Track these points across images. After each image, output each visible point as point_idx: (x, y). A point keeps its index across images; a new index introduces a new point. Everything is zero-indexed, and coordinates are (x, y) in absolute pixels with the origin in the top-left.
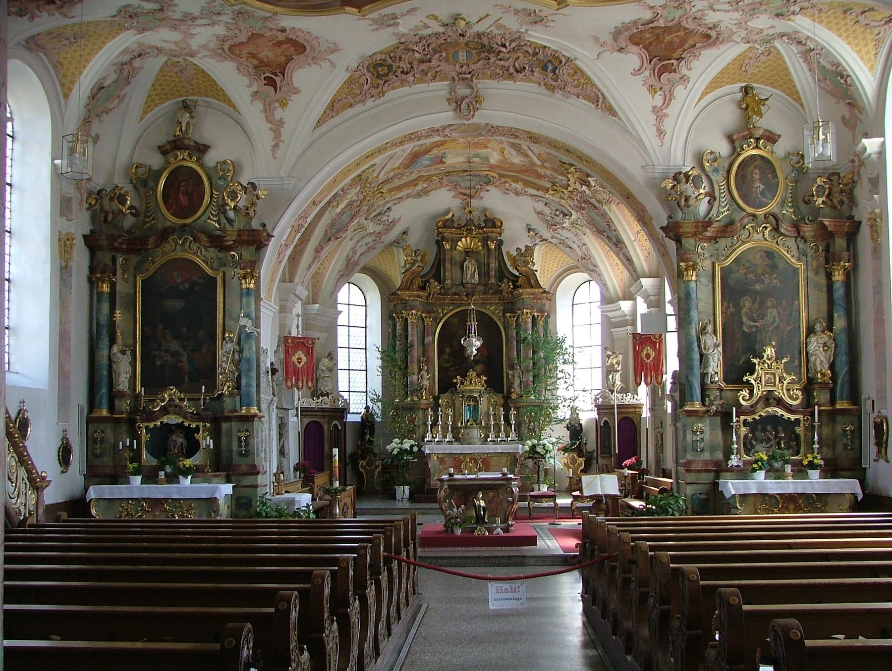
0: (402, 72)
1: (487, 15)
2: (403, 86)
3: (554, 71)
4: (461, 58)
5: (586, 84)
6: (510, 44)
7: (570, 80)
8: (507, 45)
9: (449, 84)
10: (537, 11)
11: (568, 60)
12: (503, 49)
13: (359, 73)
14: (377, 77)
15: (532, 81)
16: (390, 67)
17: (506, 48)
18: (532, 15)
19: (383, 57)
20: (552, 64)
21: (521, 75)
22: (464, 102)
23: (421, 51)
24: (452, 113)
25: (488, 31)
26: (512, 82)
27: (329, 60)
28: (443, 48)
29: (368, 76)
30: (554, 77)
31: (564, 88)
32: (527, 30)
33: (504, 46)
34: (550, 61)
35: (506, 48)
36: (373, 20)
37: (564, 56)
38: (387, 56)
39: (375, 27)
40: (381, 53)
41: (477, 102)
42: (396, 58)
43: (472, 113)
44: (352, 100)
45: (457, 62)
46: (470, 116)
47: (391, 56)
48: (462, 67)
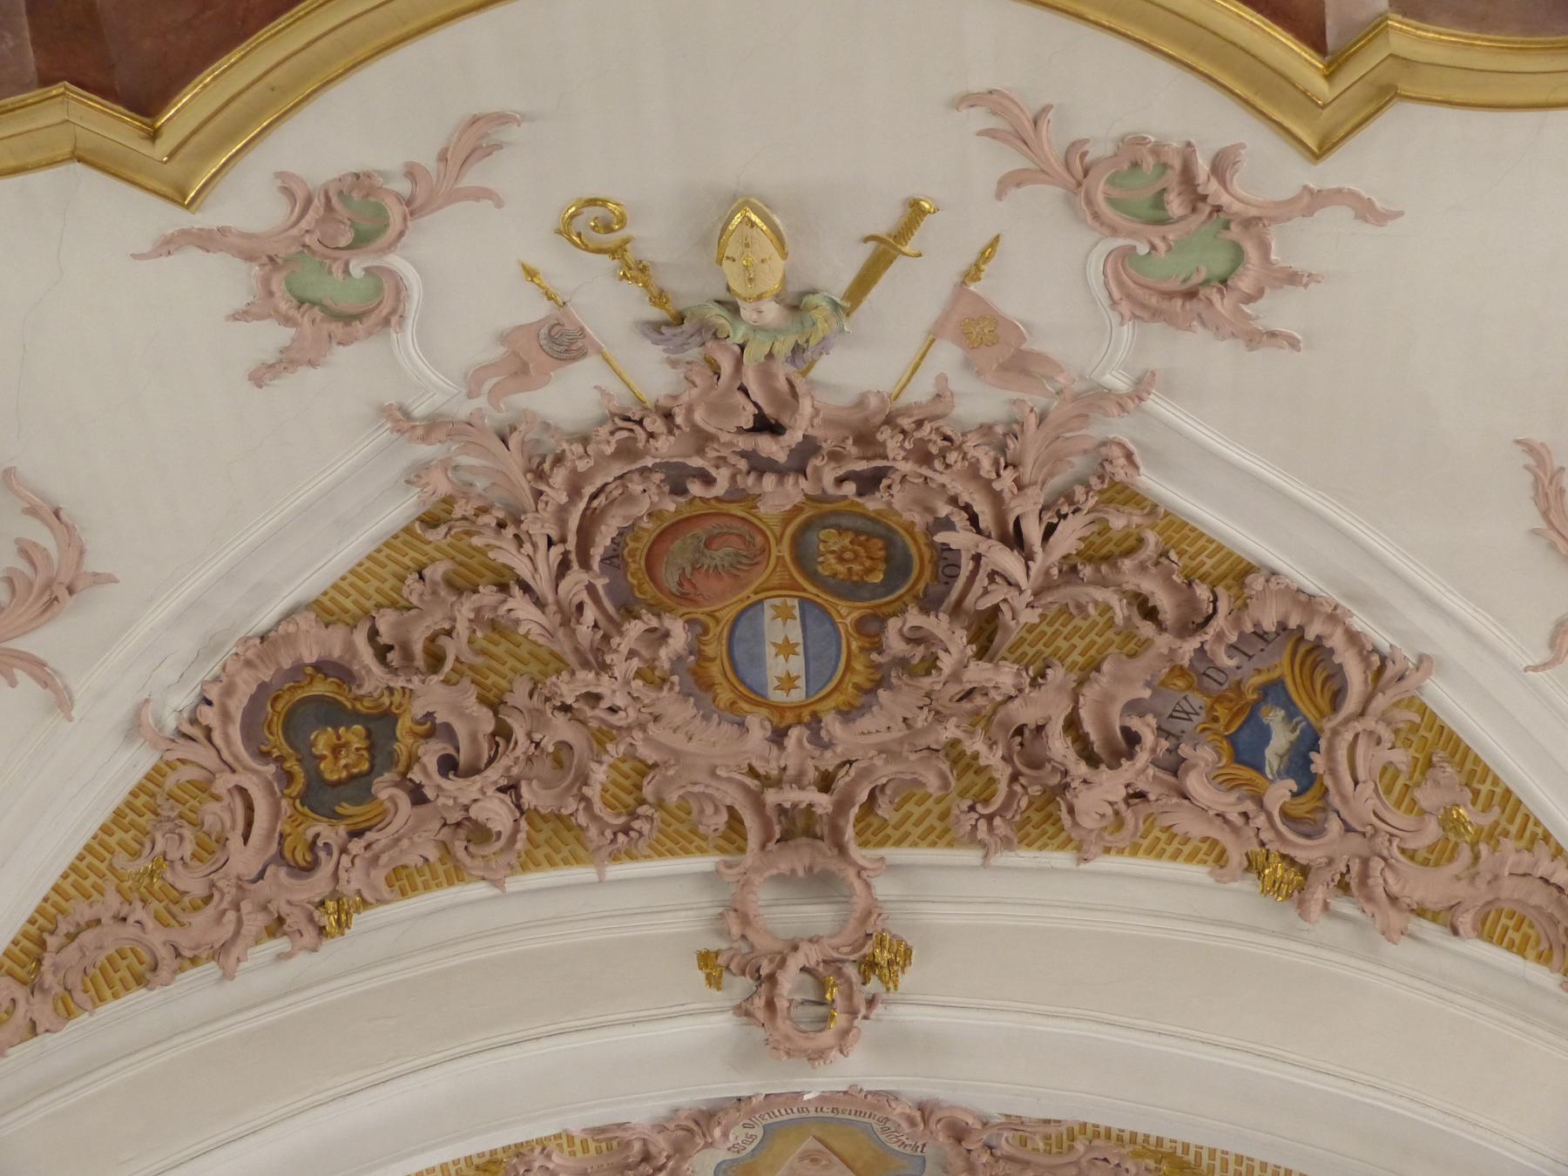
0: (448, 765)
1: (915, 212)
2: (457, 874)
3: (1299, 765)
4: (776, 666)
5: (1493, 835)
6: (1050, 531)
7: (1399, 818)
8: (1033, 531)
9: (710, 879)
10: (1203, 166)
11: (1380, 668)
12: (1010, 562)
13: (202, 754)
14: (304, 798)
15: (1170, 845)
16: (381, 723)
17: (1028, 557)
18: (1175, 206)
19: (330, 643)
20: (1292, 712)
21: (1110, 785)
22: (795, 963)
23: (542, 585)
24: (723, 1024)
25: (920, 392)
26: (1062, 859)
27: (38, 668)
28: (670, 579)
29: (256, 779)
30: (1302, 807)
31: (1364, 876)
32: (1141, 387)
33: (1015, 539)
34: (1273, 691)
35: (1028, 557)
36: (247, 249)
37: (1353, 638)
38: (360, 639)
39: (271, 337)
40: (323, 610)
41: (869, 966)
42: (408, 656)
43: (840, 1019)
44: (156, 938)
45: (757, 698)
46: (827, 1038)
47: (385, 638)
48: (778, 736)
